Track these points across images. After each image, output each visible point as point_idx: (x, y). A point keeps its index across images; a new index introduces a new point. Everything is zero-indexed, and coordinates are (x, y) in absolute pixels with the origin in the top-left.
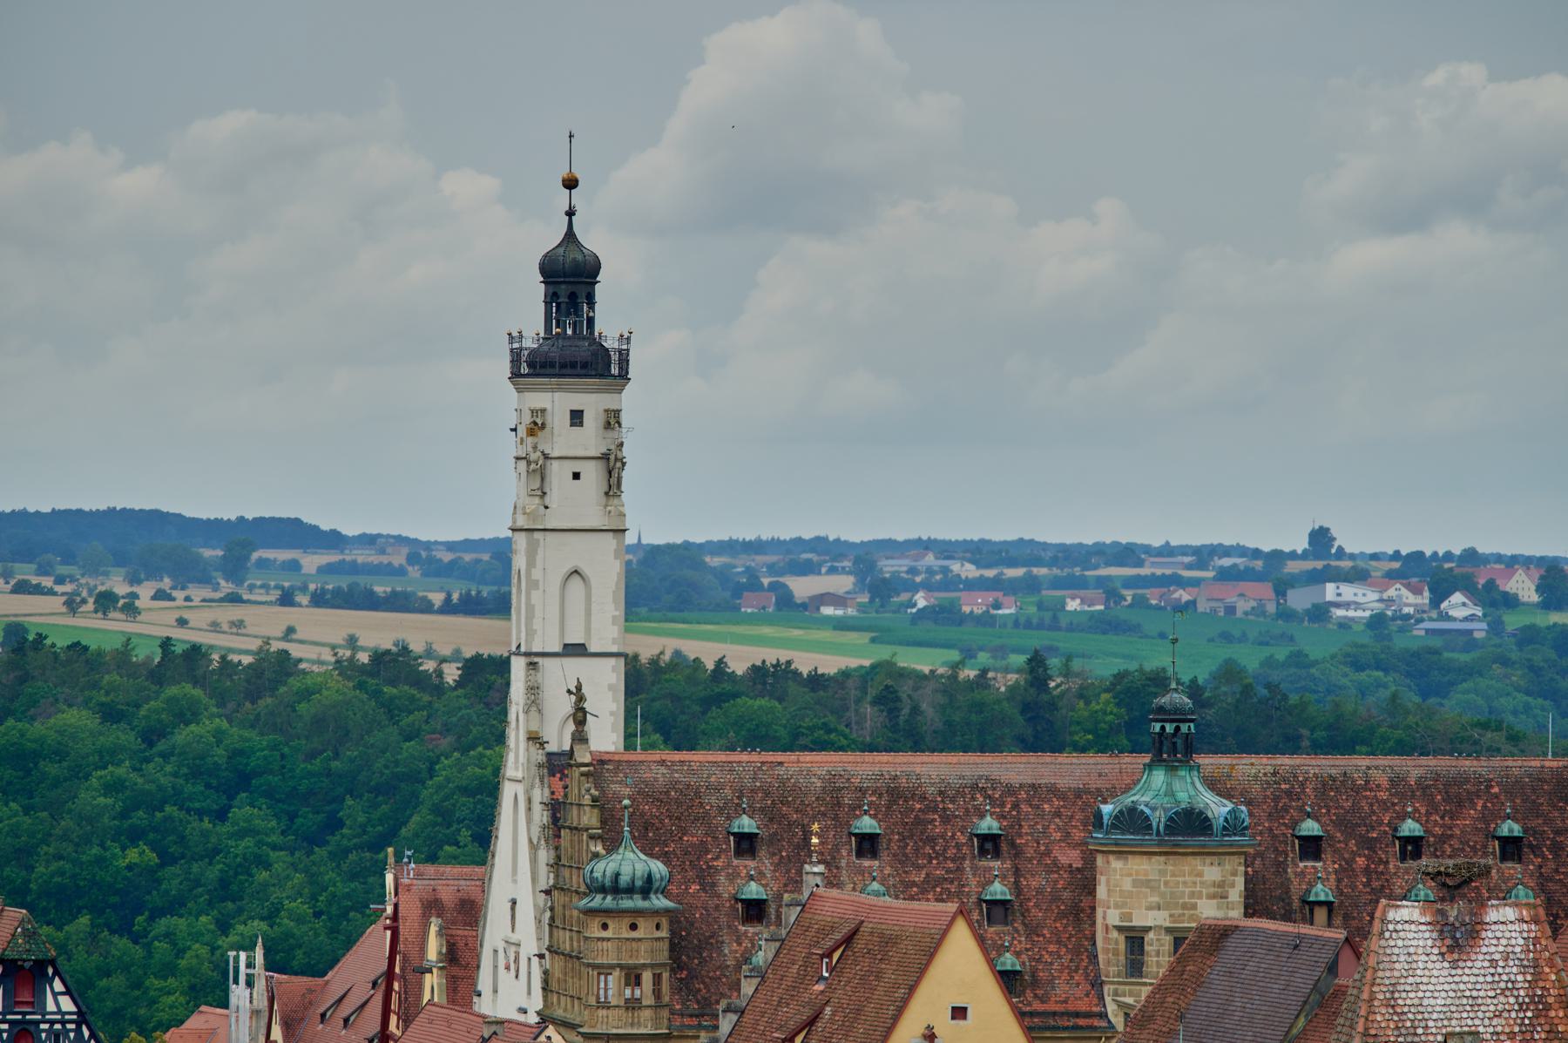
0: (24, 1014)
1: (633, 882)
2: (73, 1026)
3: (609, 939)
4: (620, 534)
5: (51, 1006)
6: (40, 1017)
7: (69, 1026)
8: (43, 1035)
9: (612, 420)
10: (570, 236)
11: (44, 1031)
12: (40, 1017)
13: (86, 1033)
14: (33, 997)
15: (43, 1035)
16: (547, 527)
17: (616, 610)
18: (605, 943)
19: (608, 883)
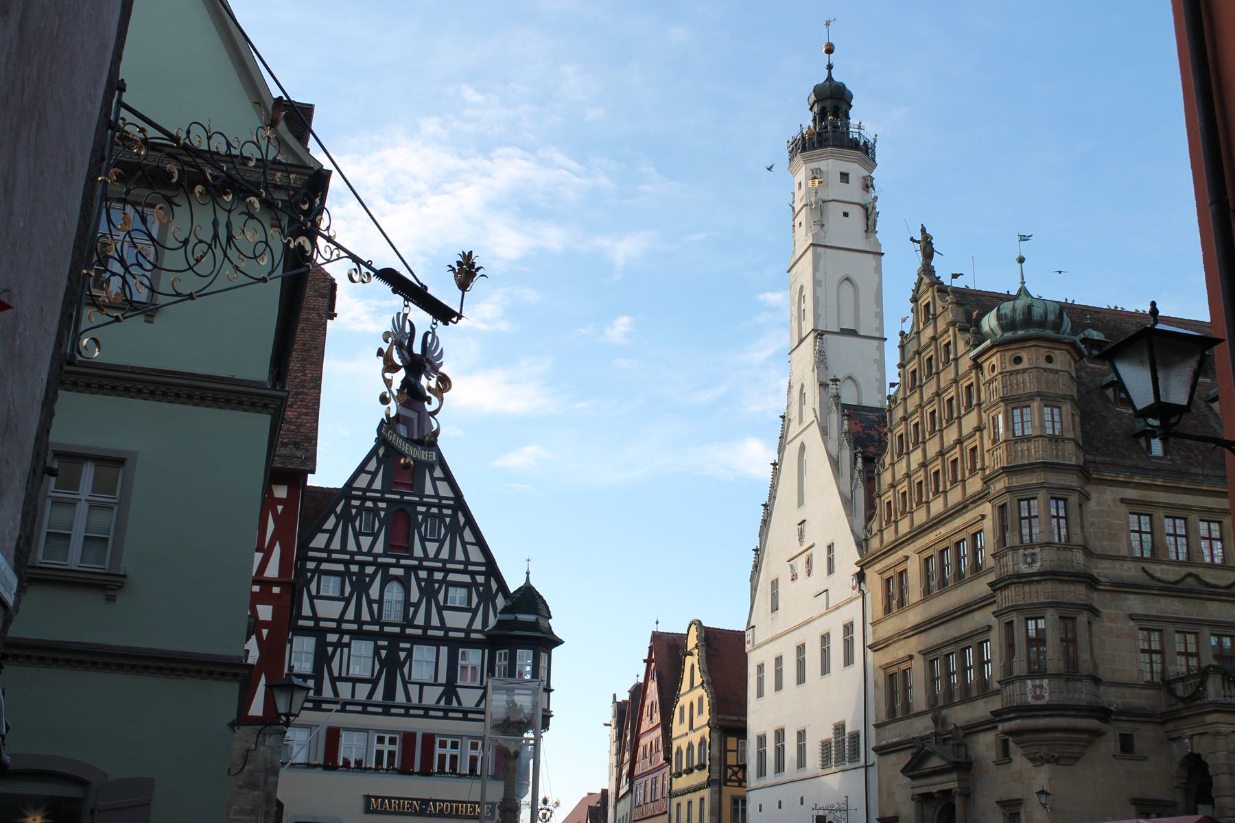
0: (403, 494)
1: (1046, 315)
2: (449, 512)
3: (1024, 371)
4: (877, 256)
5: (429, 490)
6: (417, 499)
7: (446, 511)
8: (420, 517)
9: (868, 185)
10: (830, 78)
11: (421, 513)
12: (417, 499)
13: (462, 520)
14: (413, 480)
15: (420, 517)
16: (827, 244)
17: (877, 307)
18: (1020, 377)
19: (1019, 316)
